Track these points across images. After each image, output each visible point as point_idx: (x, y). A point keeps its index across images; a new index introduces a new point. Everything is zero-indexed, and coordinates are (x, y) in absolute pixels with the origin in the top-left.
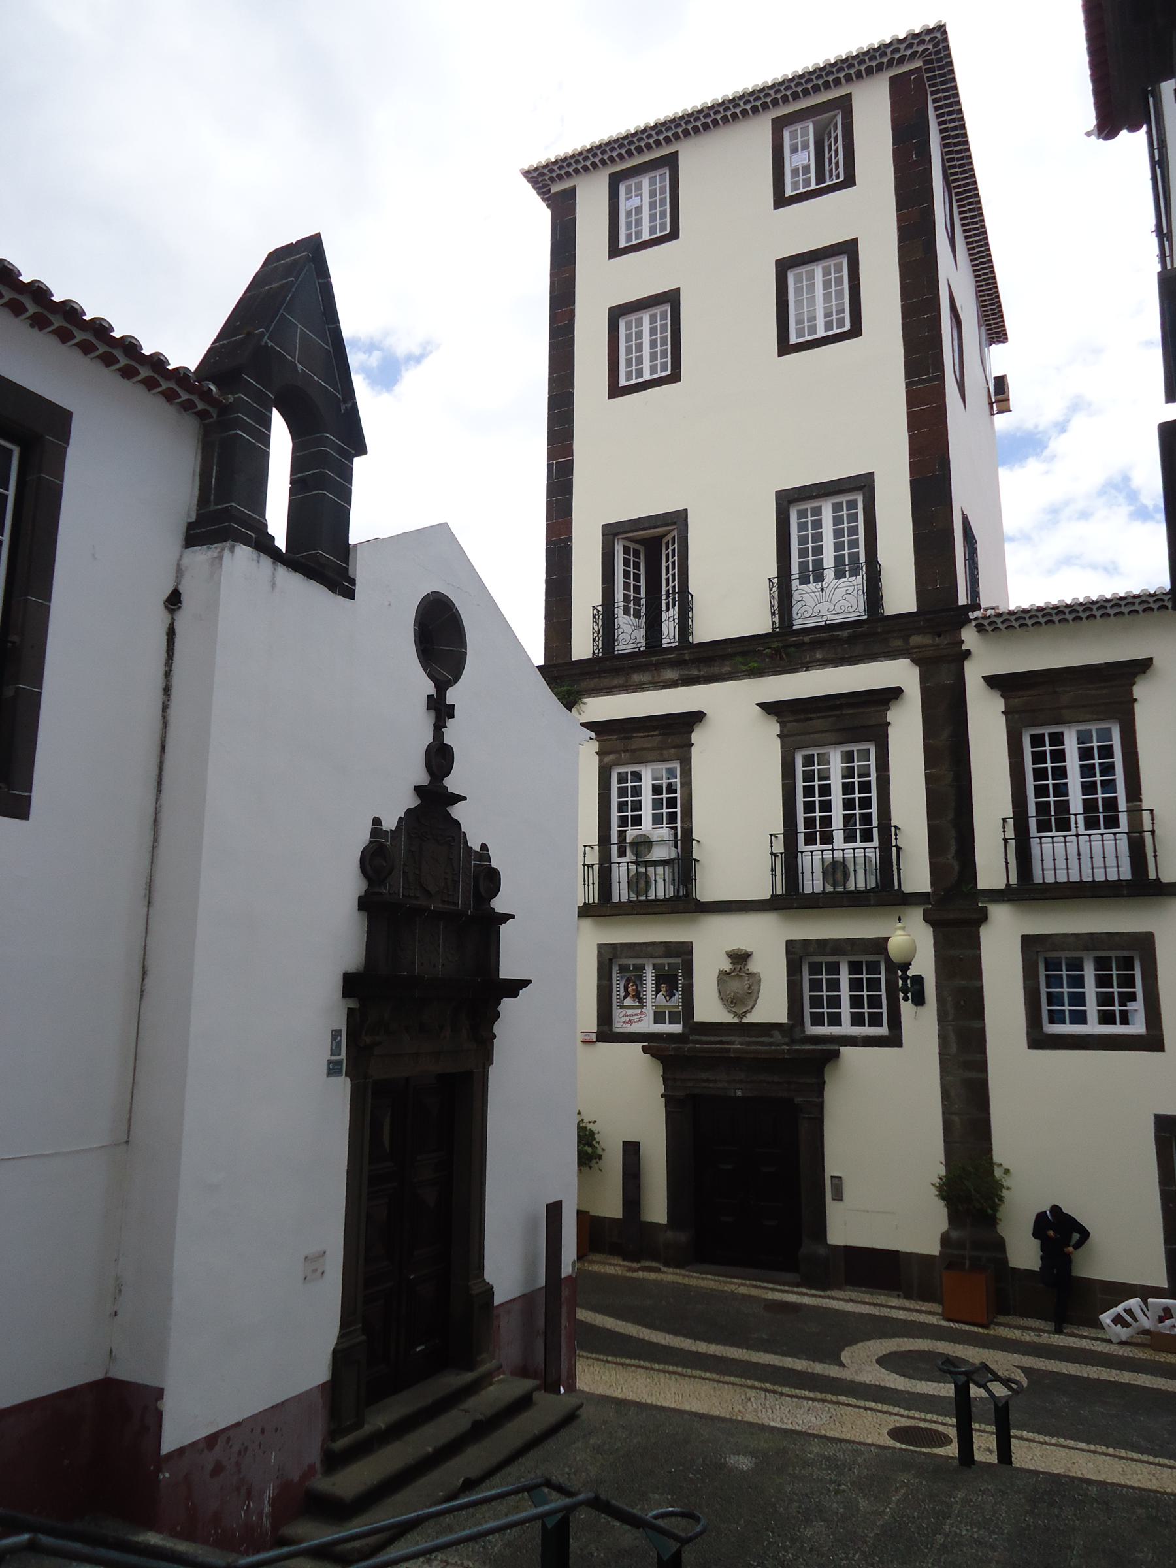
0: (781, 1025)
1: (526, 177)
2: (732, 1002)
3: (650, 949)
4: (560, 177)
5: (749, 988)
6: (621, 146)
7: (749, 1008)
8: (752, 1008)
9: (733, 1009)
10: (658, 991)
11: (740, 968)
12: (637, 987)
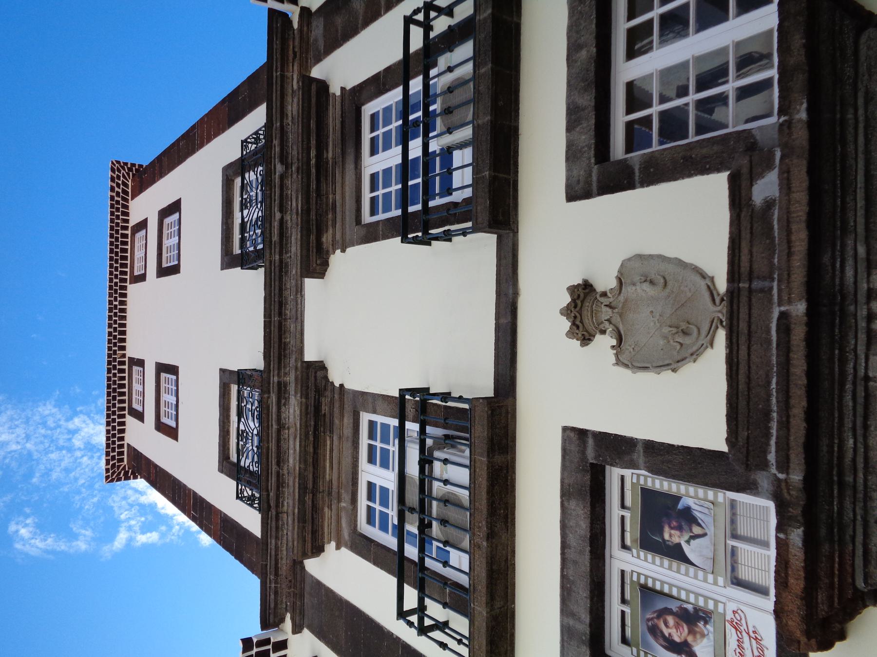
0: (734, 182)
1: (112, 481)
2: (685, 333)
3: (572, 540)
4: (122, 453)
5: (652, 282)
6: (114, 398)
7: (702, 284)
8: (703, 275)
9: (704, 332)
10: (677, 554)
11: (609, 306)
12: (667, 611)
